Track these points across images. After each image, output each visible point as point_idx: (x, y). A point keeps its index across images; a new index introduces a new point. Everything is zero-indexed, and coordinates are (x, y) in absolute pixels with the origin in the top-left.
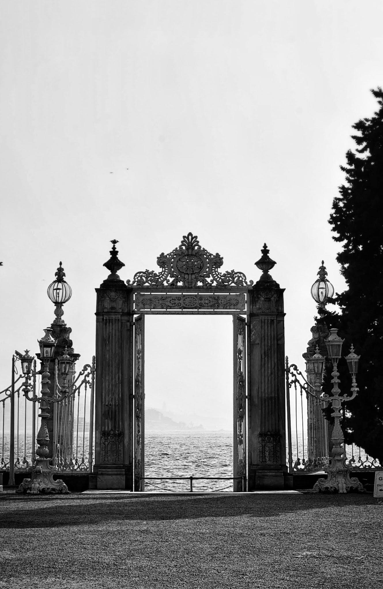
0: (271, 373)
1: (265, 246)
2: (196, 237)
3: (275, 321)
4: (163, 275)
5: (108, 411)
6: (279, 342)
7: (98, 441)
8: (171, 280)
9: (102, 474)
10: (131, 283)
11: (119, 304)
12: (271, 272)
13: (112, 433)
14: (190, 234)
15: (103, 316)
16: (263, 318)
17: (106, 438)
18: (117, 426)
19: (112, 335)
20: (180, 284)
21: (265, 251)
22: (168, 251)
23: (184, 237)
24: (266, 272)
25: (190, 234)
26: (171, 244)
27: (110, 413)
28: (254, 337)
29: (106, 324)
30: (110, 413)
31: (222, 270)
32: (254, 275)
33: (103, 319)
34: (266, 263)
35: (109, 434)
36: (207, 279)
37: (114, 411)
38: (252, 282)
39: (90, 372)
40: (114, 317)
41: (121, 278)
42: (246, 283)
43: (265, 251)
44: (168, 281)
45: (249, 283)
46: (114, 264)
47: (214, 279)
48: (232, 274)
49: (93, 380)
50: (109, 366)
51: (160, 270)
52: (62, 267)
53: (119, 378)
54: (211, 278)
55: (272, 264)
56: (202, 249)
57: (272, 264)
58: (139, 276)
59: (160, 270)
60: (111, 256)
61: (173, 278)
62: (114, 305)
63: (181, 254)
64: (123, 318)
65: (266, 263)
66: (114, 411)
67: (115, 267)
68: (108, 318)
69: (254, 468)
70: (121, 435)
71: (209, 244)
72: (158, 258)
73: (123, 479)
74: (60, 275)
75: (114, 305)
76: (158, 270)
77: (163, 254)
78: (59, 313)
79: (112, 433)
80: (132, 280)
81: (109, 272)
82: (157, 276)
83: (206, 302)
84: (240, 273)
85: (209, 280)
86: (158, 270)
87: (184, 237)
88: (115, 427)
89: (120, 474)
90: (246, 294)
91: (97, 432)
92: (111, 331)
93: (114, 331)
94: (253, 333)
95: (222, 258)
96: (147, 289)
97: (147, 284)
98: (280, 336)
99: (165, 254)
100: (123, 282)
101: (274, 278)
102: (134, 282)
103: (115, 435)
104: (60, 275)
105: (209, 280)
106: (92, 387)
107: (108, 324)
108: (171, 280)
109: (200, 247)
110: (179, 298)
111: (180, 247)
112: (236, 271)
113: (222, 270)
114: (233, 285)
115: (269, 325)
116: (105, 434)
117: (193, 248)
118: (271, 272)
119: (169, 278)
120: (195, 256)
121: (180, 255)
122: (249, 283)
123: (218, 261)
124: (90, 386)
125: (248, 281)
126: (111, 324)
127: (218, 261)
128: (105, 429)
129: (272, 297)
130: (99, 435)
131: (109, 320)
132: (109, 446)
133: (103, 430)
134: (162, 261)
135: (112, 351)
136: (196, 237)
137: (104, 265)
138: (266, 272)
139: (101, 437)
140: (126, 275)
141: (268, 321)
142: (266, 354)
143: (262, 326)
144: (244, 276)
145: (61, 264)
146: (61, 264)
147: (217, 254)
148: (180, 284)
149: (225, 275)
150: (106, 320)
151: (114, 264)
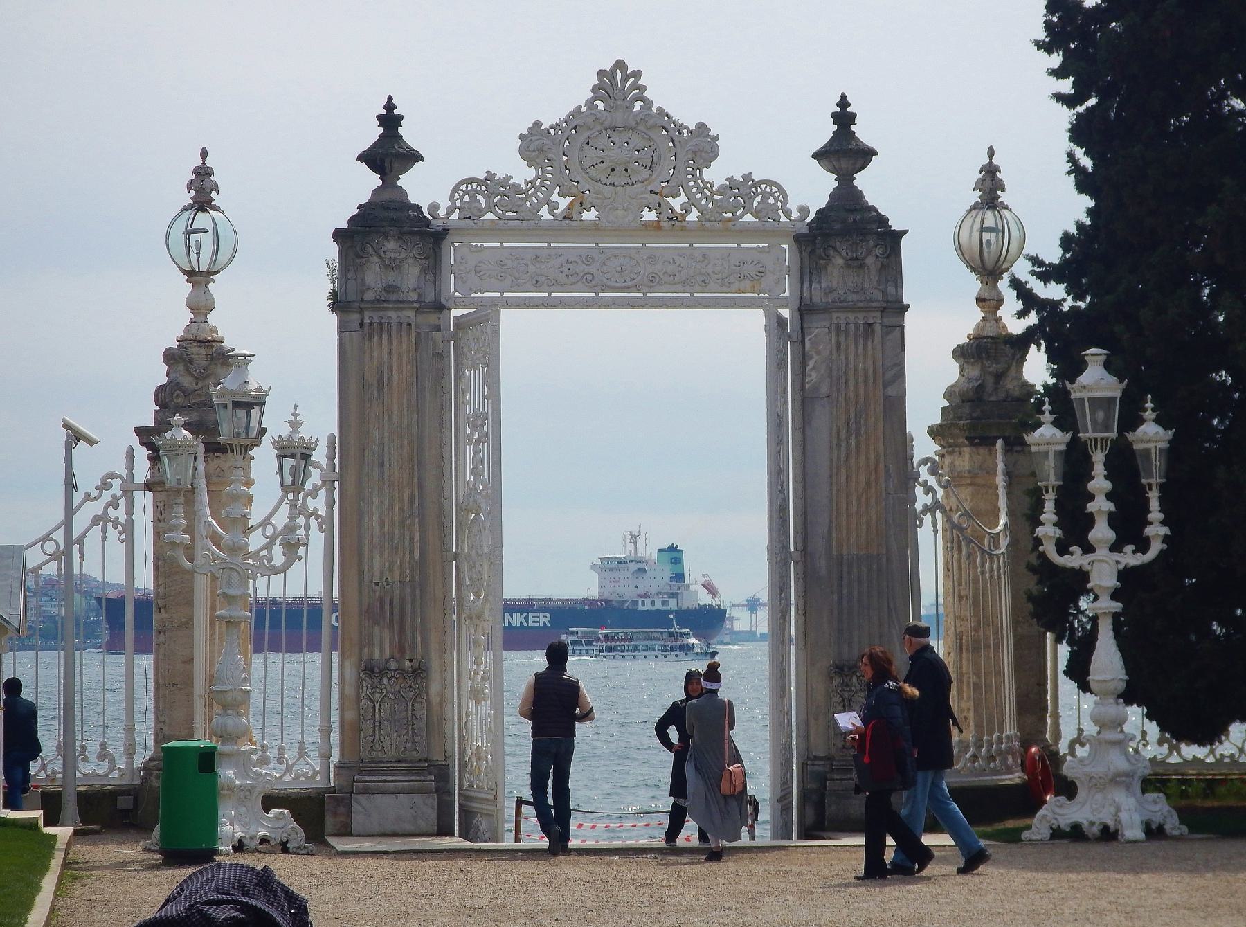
0: (868, 484)
1: (843, 103)
2: (637, 74)
3: (878, 327)
4: (538, 190)
5: (381, 600)
6: (891, 391)
7: (350, 690)
8: (564, 203)
9: (366, 791)
10: (442, 212)
11: (411, 276)
12: (862, 180)
13: (393, 665)
14: (620, 65)
15: (361, 311)
16: (840, 317)
17: (376, 681)
18: (409, 645)
19: (390, 368)
20: (590, 216)
21: (844, 118)
23: (601, 74)
24: (845, 179)
25: (620, 65)
26: (565, 94)
27: (387, 607)
28: (814, 375)
29: (371, 337)
30: (387, 607)
31: (716, 174)
32: (812, 189)
33: (361, 325)
34: (845, 151)
35: (383, 671)
36: (670, 200)
37: (397, 601)
38: (804, 210)
39: (320, 483)
40: (393, 315)
41: (413, 198)
42: (788, 213)
43: (844, 118)
44: (553, 207)
45: (795, 214)
46: (389, 154)
47: (692, 201)
48: (743, 188)
49: (330, 504)
50: (381, 464)
52: (209, 162)
53: (411, 502)
54: (683, 198)
55: (865, 155)
56: (654, 109)
57: (865, 155)
58: (466, 192)
59: (531, 173)
60: (381, 130)
61: (569, 200)
62: (392, 277)
63: (590, 120)
64: (421, 319)
65: (845, 151)
66: (397, 601)
67: (396, 165)
68: (376, 320)
69: (819, 767)
70: (419, 672)
71: (674, 94)
72: (522, 137)
73: (427, 807)
74: (202, 192)
75: (392, 277)
76: (521, 173)
77: (537, 124)
78: (200, 307)
79: (393, 665)
80: (445, 204)
81: (375, 180)
82: (520, 191)
83: (670, 268)
84: (771, 183)
85: (676, 203)
86: (521, 173)
87: (601, 74)
88: (402, 650)
89: (420, 791)
90: (786, 247)
91: (348, 664)
92: (386, 357)
93: (394, 359)
94: (811, 364)
96: (492, 230)
97: (489, 216)
98: (889, 375)
99: (545, 126)
100: (419, 208)
101: (871, 198)
102: (450, 211)
103: (403, 672)
104: (202, 192)
105: (676, 203)
106: (326, 525)
107: (376, 337)
109: (647, 103)
110: (587, 258)
111: (590, 104)
112: (757, 178)
113: (716, 174)
114: (748, 218)
115: (861, 341)
116: (373, 671)
117: (630, 107)
118: (862, 180)
119: (555, 197)
122: (795, 214)
123: (702, 145)
124: (320, 525)
125: (793, 206)
126: (386, 337)
127: (702, 145)
128: (371, 654)
129: (869, 254)
130: (351, 674)
131: (381, 324)
132: (386, 706)
133: (366, 656)
134: (535, 144)
135: (390, 417)
136: (637, 74)
137: (360, 158)
138: (845, 179)
139: (361, 680)
140: (423, 188)
141: (857, 329)
142: (853, 427)
143: (838, 343)
144: (782, 191)
145: (204, 154)
146: (204, 154)
147: (702, 126)
148: (590, 216)
149: (722, 191)
150: (371, 324)
151: (389, 154)
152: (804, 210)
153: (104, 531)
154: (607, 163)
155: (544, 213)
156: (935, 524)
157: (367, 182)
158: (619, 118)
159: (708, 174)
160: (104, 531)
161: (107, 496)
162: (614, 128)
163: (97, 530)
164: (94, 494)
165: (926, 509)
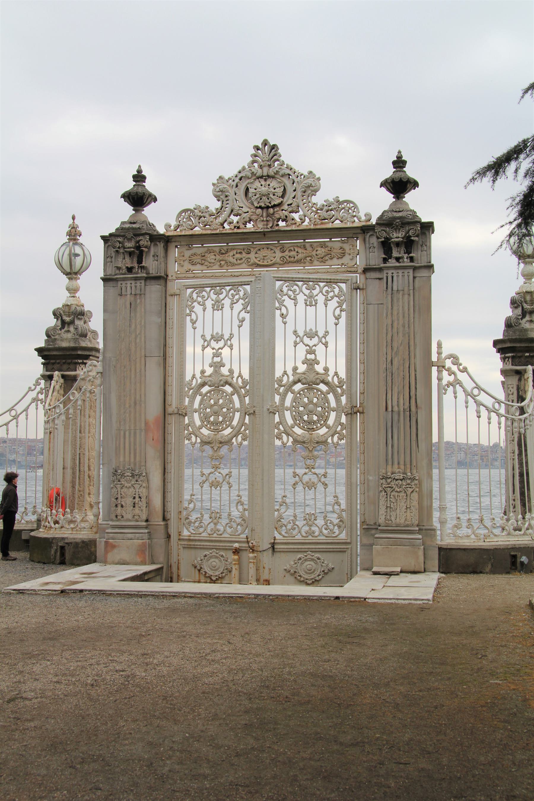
2: (274, 147)
14: (265, 143)
20: (249, 226)
22: (230, 171)
25: (265, 143)
26: (236, 159)
31: (319, 199)
32: (375, 203)
36: (294, 215)
38: (368, 217)
45: (363, 218)
51: (218, 205)
59: (218, 205)
71: (296, 157)
72: (214, 185)
77: (221, 178)
80: (173, 223)
85: (296, 216)
86: (214, 205)
95: (319, 179)
102: (177, 227)
105: (296, 216)
108: (235, 219)
109: (283, 164)
112: (341, 199)
113: (319, 199)
120: (273, 177)
121: (249, 178)
144: (355, 206)
147: (310, 172)
152: (368, 217)
153: (37, 405)
154: (258, 196)
155: (226, 225)
156: (455, 393)
157: (126, 211)
158: (265, 171)
159: (314, 199)
160: (37, 405)
161: (38, 388)
162: (262, 177)
163: (34, 404)
164: (33, 387)
165: (449, 384)
